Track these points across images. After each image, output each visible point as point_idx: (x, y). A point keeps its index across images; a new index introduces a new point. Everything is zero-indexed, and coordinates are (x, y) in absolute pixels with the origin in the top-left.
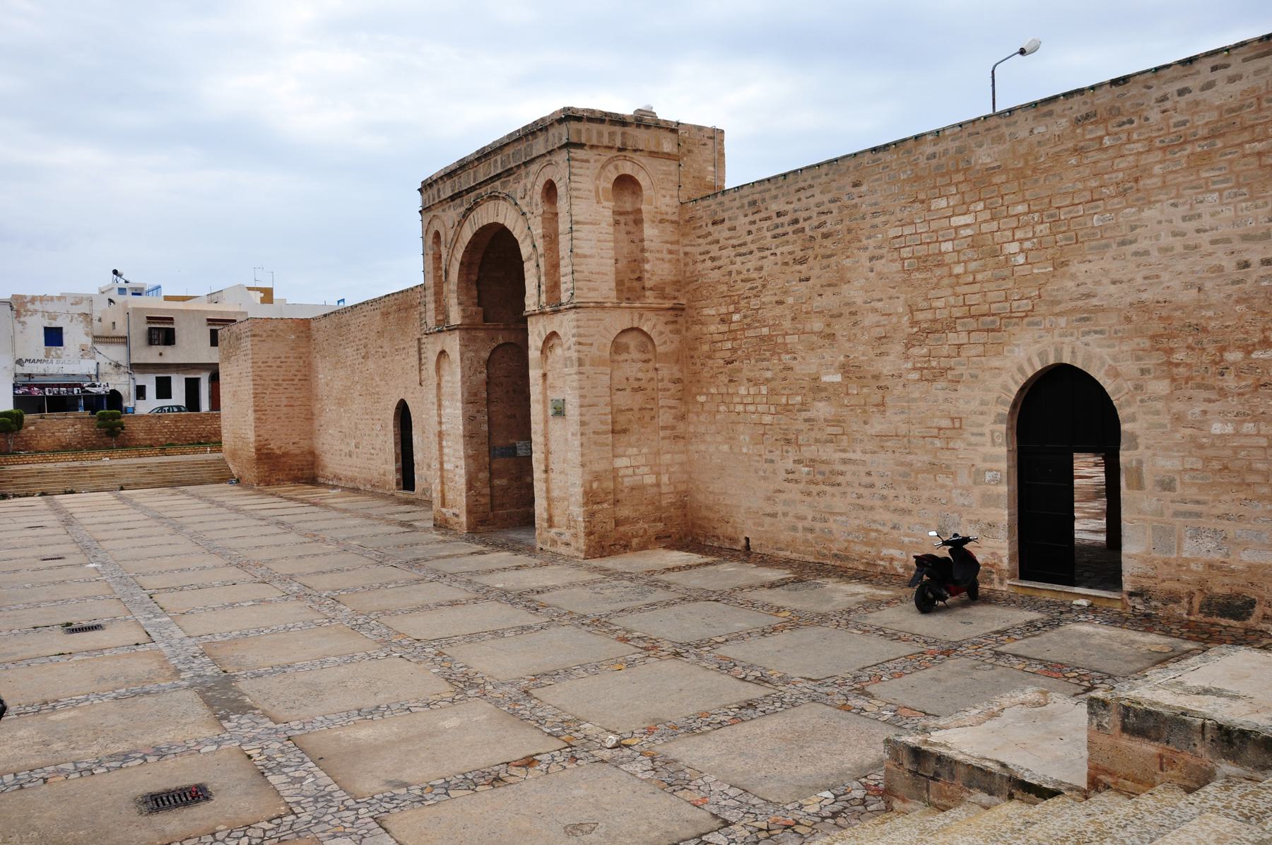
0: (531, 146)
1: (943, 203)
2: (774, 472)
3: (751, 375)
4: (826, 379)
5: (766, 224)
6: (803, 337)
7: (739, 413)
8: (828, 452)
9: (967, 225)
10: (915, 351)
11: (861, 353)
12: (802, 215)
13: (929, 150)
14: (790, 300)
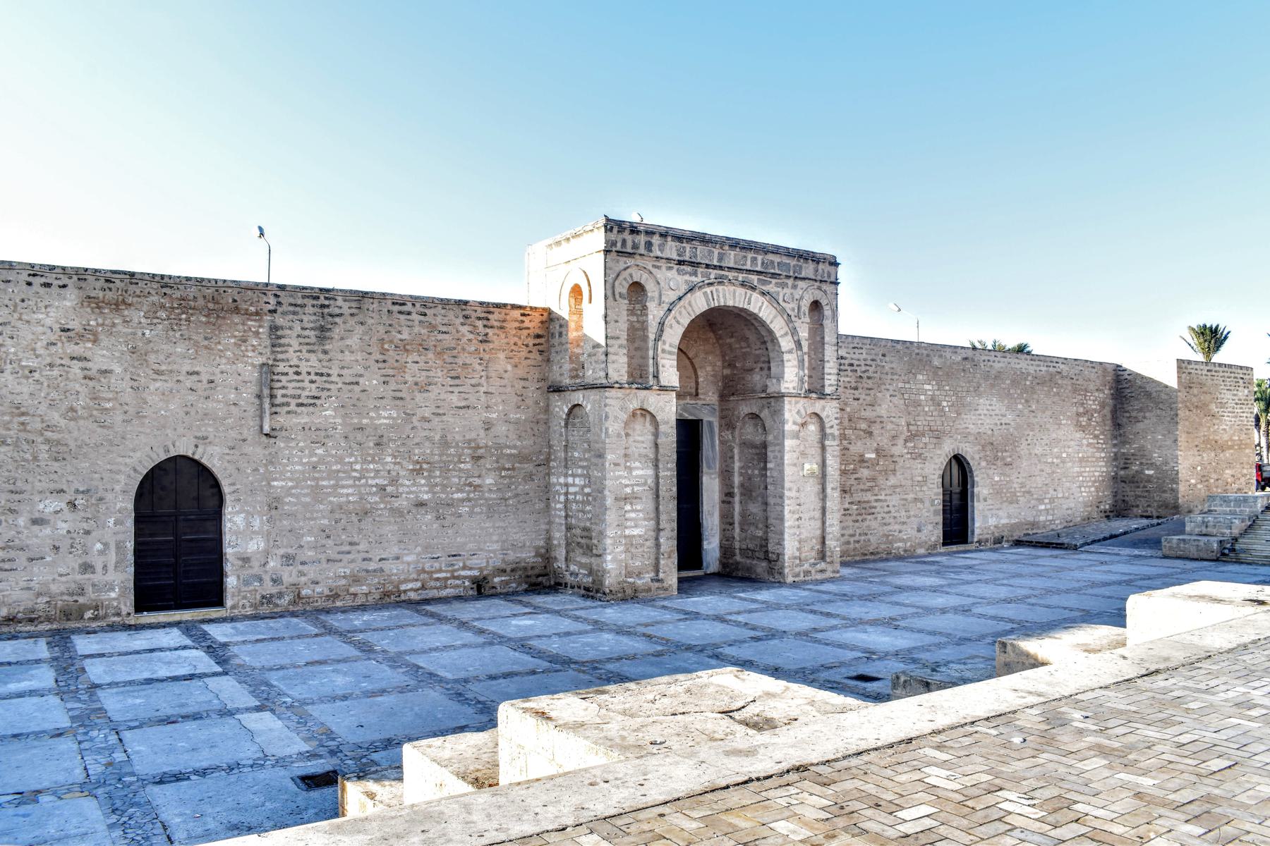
4: (867, 456)
11: (885, 442)
12: (856, 363)
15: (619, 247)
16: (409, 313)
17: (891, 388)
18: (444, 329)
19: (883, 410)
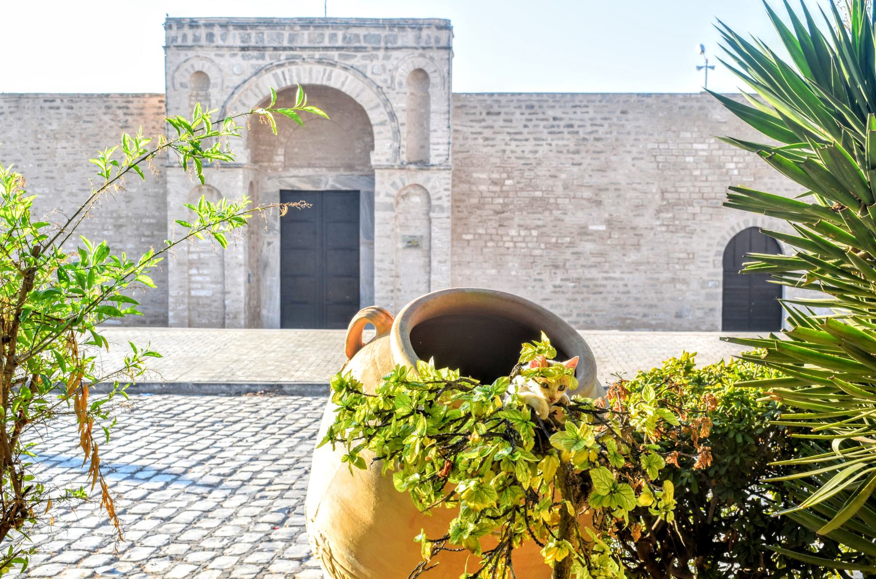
0: (395, 38)
1: (688, 135)
2: (543, 287)
3: (522, 222)
4: (592, 228)
5: (542, 123)
6: (573, 200)
7: (508, 248)
8: (594, 273)
9: (703, 150)
10: (663, 215)
11: (622, 212)
12: (576, 123)
13: (681, 104)
14: (563, 176)
15: (179, 42)
16: (58, 108)
17: (634, 150)
18: (88, 119)
19: (619, 176)
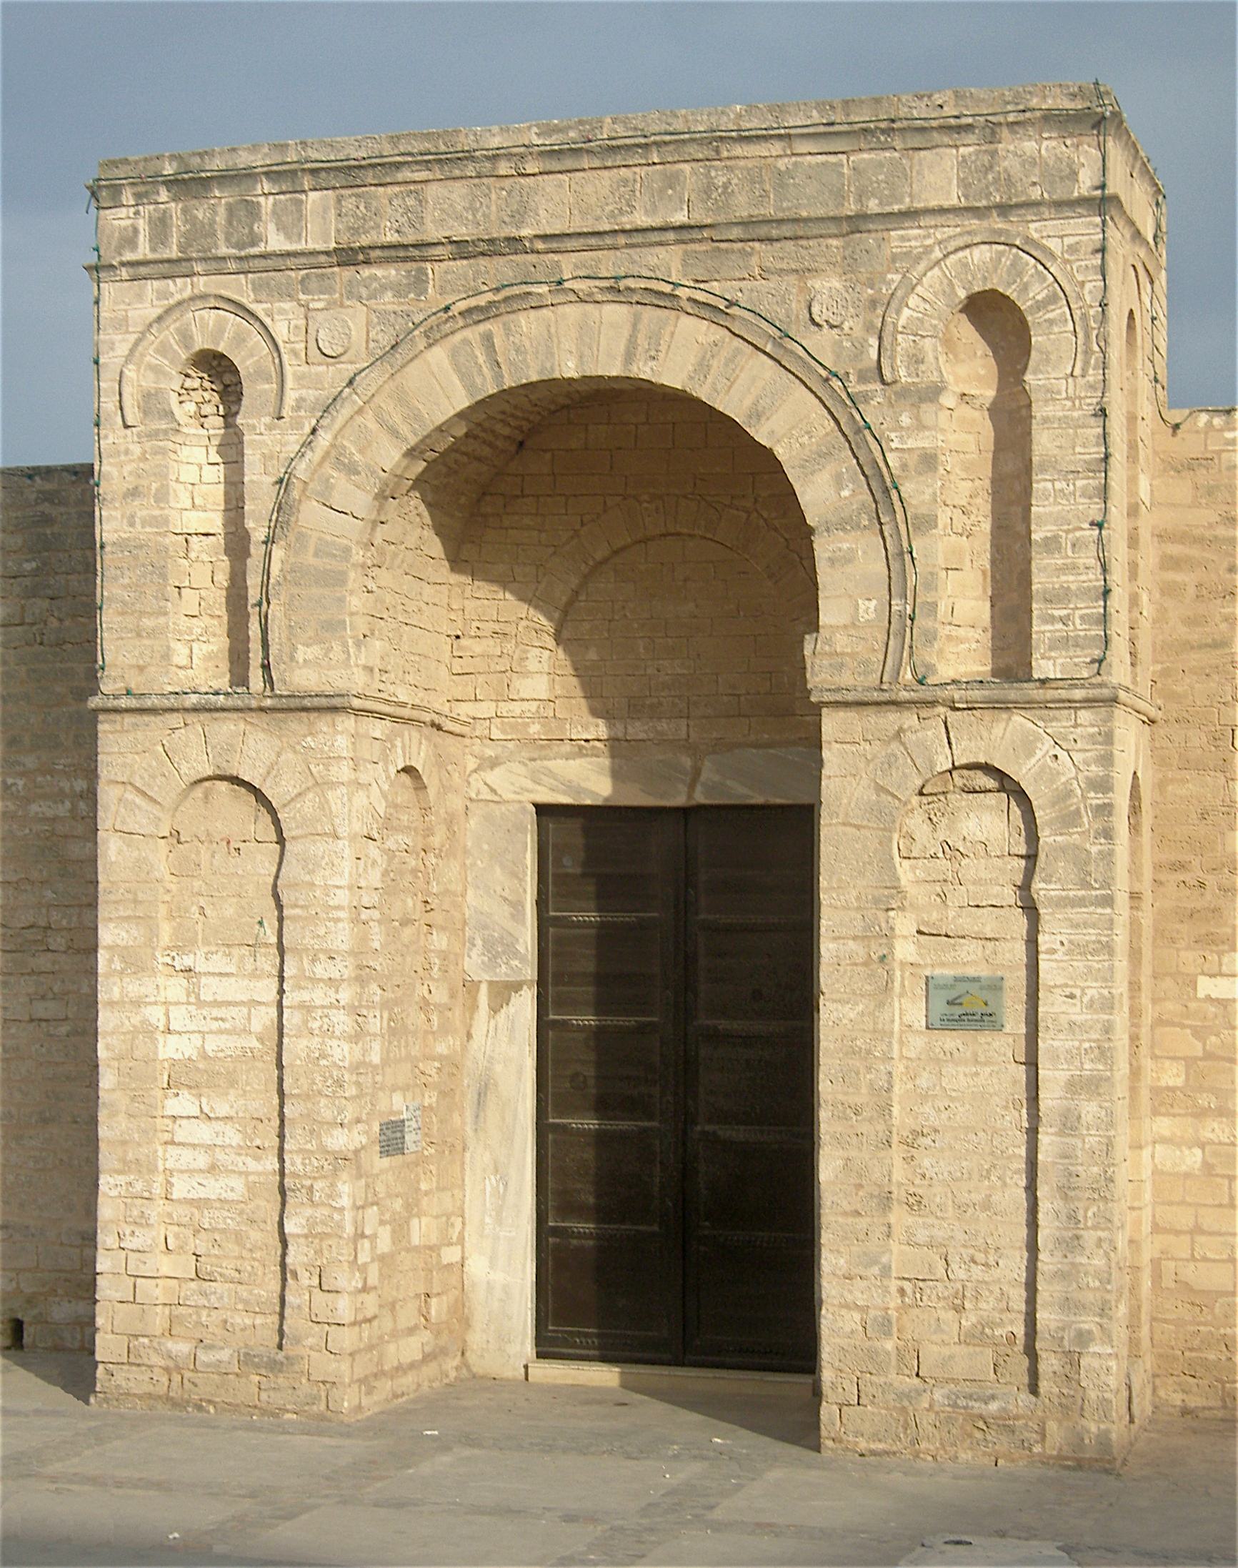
15: (143, 250)
